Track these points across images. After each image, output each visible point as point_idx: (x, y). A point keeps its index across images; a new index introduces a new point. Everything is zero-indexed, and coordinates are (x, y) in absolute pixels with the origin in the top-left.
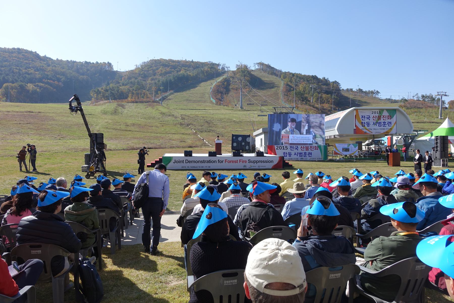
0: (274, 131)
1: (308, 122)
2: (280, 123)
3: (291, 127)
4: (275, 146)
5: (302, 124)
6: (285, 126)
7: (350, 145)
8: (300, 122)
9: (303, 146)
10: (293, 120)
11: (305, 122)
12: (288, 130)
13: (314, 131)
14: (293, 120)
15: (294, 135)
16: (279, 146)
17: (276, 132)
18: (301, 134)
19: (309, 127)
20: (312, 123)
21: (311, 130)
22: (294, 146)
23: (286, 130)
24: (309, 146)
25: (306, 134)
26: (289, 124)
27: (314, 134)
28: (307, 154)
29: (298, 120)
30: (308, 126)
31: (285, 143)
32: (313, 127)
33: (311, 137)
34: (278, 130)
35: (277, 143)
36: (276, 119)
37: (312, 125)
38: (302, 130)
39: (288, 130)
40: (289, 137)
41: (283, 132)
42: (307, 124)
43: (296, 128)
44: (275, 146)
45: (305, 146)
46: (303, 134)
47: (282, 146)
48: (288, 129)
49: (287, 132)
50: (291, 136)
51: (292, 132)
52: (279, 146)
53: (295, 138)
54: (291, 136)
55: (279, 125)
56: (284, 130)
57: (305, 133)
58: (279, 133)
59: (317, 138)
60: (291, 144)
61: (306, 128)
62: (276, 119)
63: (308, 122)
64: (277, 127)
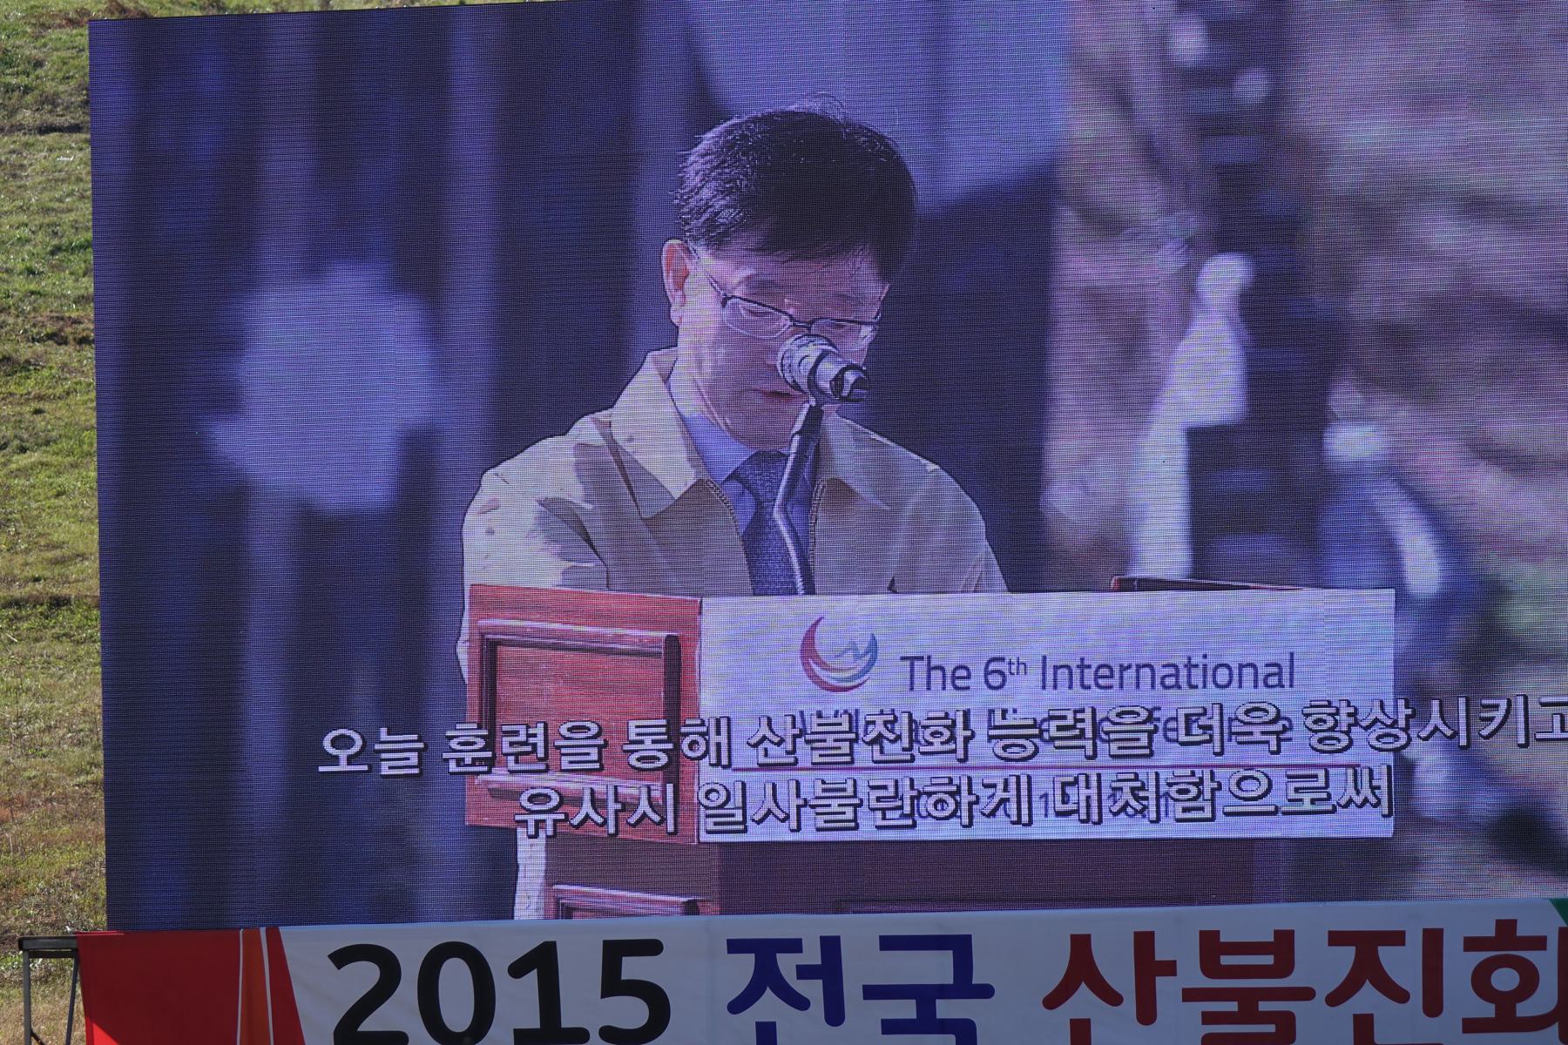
0: (233, 498)
1: (1251, 191)
2: (419, 274)
3: (751, 385)
4: (307, 948)
5: (1082, 266)
6: (565, 355)
8: (1027, 209)
9: (1112, 930)
10: (814, 190)
11: (1145, 202)
12: (674, 473)
13: (1441, 463)
14: (814, 190)
15: (847, 613)
16: (409, 943)
17: (316, 529)
18: (1030, 560)
19: (1296, 355)
20: (1380, 216)
21: (1353, 442)
22: (859, 932)
23: (614, 472)
24: (1310, 921)
25: (1205, 573)
26: (703, 292)
27: (1424, 568)
29: (963, 161)
30: (1260, 314)
31: (574, 854)
32: (1404, 361)
33: (1335, 638)
34: (363, 482)
35: (353, 858)
36: (287, 166)
37: (1383, 290)
38: (1067, 446)
39: (674, 473)
40: (676, 662)
41: (506, 536)
42: (1226, 275)
43: (897, 399)
44: (307, 948)
45: (1178, 929)
46: (1106, 564)
47: (499, 944)
48: (657, 420)
49: (616, 527)
50: (745, 652)
51: (770, 517)
52: (409, 943)
53: (863, 680)
54: (745, 652)
55: (397, 322)
56: (550, 467)
57: (1163, 542)
58: (391, 562)
59: (1534, 688)
60: (755, 875)
61: (1204, 377)
62: (287, 166)
63: (1251, 191)
64: (326, 380)
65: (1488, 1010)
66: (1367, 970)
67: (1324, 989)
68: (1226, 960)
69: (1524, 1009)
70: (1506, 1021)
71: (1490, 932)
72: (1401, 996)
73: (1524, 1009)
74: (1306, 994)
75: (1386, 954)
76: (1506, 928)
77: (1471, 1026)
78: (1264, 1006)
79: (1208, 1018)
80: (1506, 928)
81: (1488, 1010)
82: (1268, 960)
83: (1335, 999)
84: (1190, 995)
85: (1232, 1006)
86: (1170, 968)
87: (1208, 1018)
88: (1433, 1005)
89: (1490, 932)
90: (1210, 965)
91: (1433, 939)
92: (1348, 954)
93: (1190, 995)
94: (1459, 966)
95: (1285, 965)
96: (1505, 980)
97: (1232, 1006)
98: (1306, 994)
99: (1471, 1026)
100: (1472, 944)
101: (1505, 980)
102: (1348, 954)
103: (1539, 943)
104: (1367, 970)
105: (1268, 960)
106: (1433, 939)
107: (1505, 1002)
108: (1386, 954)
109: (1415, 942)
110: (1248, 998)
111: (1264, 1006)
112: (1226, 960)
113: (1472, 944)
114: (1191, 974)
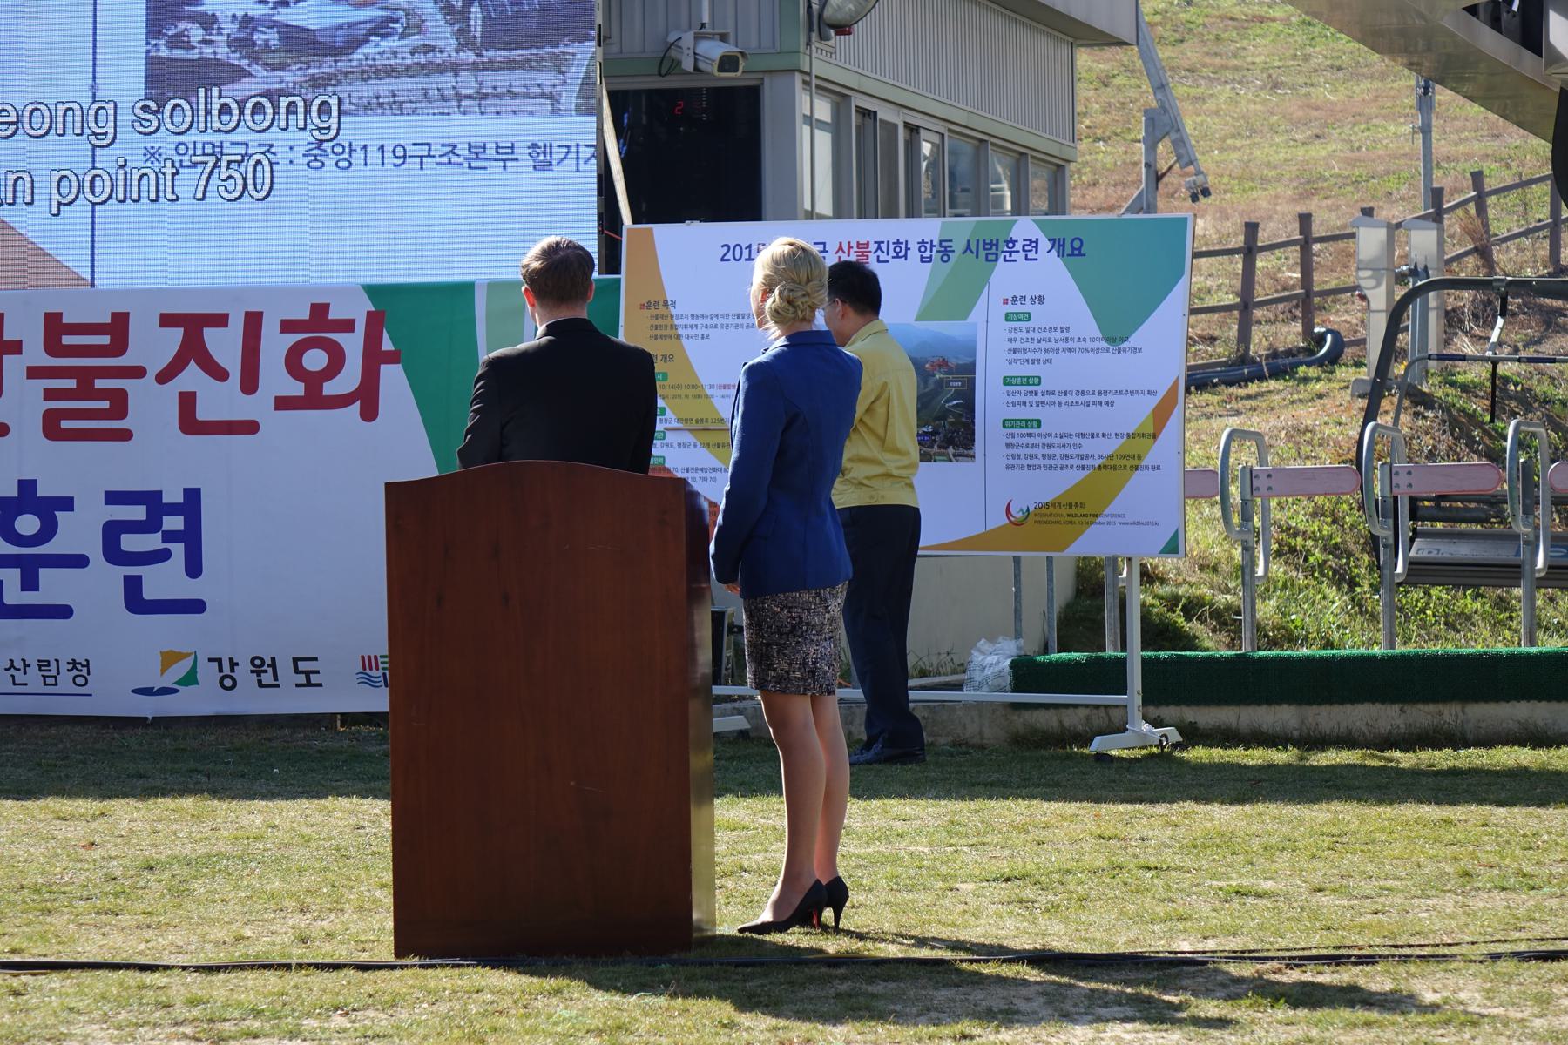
7: (992, 249)
28: (79, 531)
65: (297, 389)
66: (193, 351)
67: (155, 366)
68: (67, 340)
69: (330, 388)
70: (314, 400)
71: (306, 316)
72: (220, 374)
73: (330, 388)
74: (138, 372)
75: (211, 335)
76: (320, 310)
77: (283, 403)
78: (100, 384)
79: (50, 394)
80: (320, 310)
81: (297, 389)
82: (105, 340)
83: (164, 377)
84: (34, 373)
85: (71, 384)
86: (16, 348)
87: (50, 394)
88: (250, 384)
89: (306, 316)
90: (53, 345)
91: (253, 322)
92: (176, 335)
93: (34, 373)
94: (275, 346)
95: (119, 345)
96: (315, 360)
97: (71, 384)
98: (138, 372)
99: (283, 403)
100: (288, 326)
101: (315, 360)
102: (176, 335)
103: (347, 326)
104: (193, 351)
105: (105, 340)
106: (253, 322)
107: (314, 381)
108: (211, 335)
109: (237, 325)
110: (86, 377)
111: (100, 384)
112: (67, 340)
113: (288, 326)
114: (36, 354)
